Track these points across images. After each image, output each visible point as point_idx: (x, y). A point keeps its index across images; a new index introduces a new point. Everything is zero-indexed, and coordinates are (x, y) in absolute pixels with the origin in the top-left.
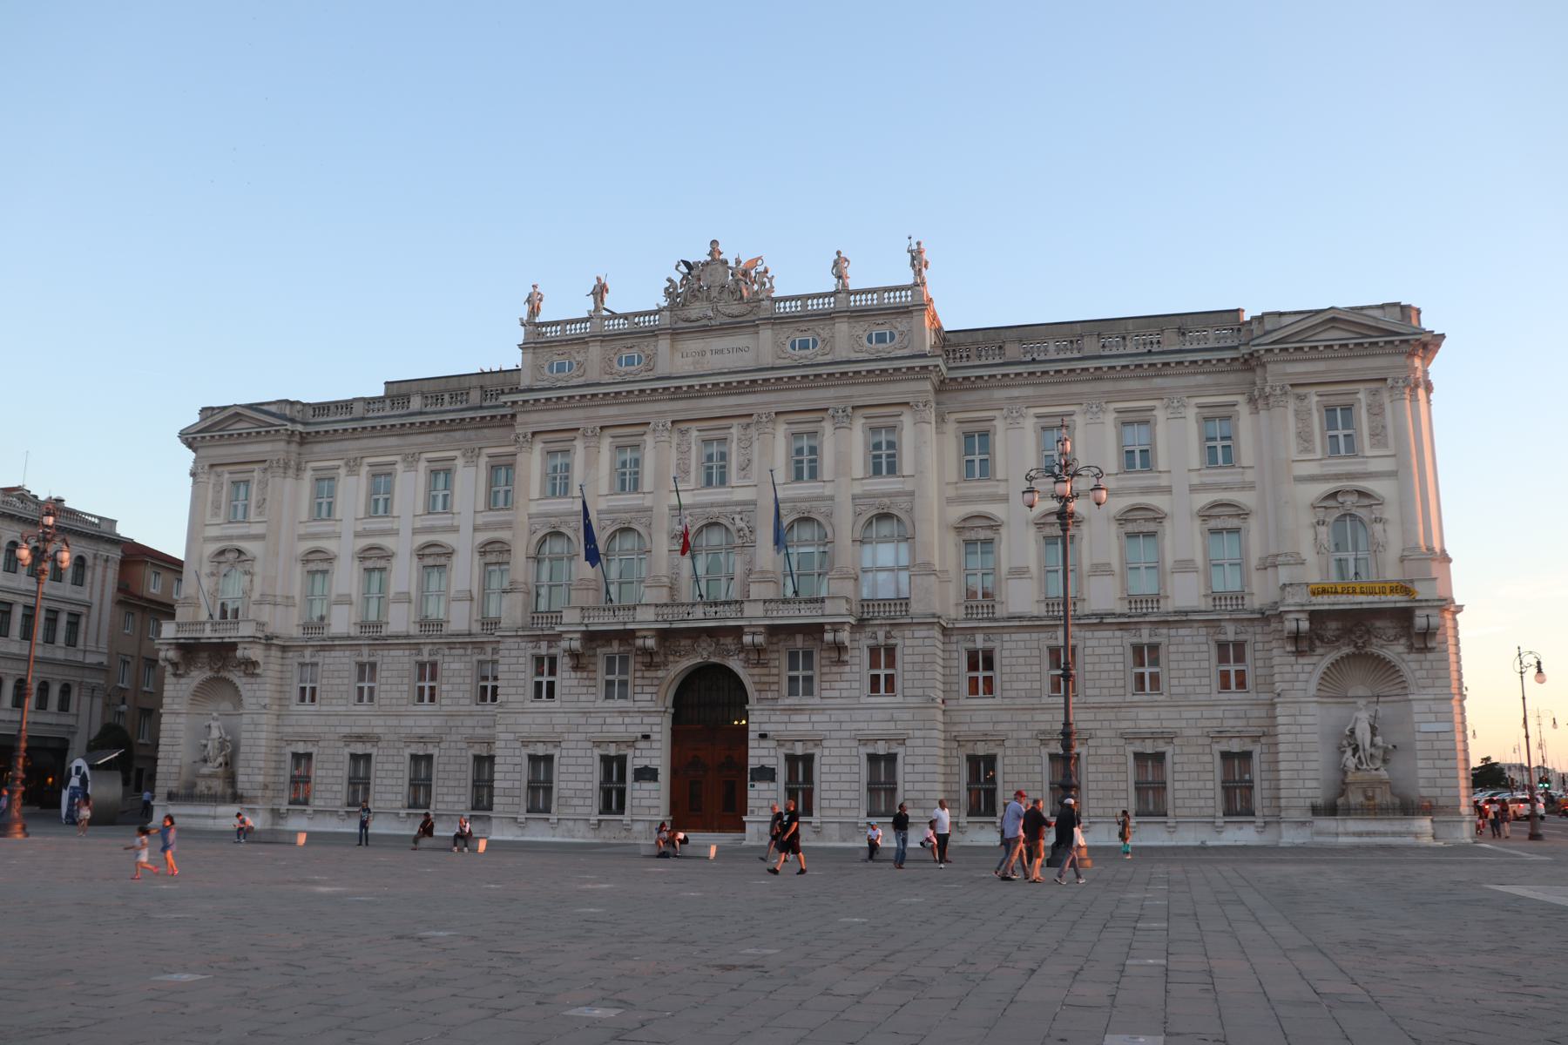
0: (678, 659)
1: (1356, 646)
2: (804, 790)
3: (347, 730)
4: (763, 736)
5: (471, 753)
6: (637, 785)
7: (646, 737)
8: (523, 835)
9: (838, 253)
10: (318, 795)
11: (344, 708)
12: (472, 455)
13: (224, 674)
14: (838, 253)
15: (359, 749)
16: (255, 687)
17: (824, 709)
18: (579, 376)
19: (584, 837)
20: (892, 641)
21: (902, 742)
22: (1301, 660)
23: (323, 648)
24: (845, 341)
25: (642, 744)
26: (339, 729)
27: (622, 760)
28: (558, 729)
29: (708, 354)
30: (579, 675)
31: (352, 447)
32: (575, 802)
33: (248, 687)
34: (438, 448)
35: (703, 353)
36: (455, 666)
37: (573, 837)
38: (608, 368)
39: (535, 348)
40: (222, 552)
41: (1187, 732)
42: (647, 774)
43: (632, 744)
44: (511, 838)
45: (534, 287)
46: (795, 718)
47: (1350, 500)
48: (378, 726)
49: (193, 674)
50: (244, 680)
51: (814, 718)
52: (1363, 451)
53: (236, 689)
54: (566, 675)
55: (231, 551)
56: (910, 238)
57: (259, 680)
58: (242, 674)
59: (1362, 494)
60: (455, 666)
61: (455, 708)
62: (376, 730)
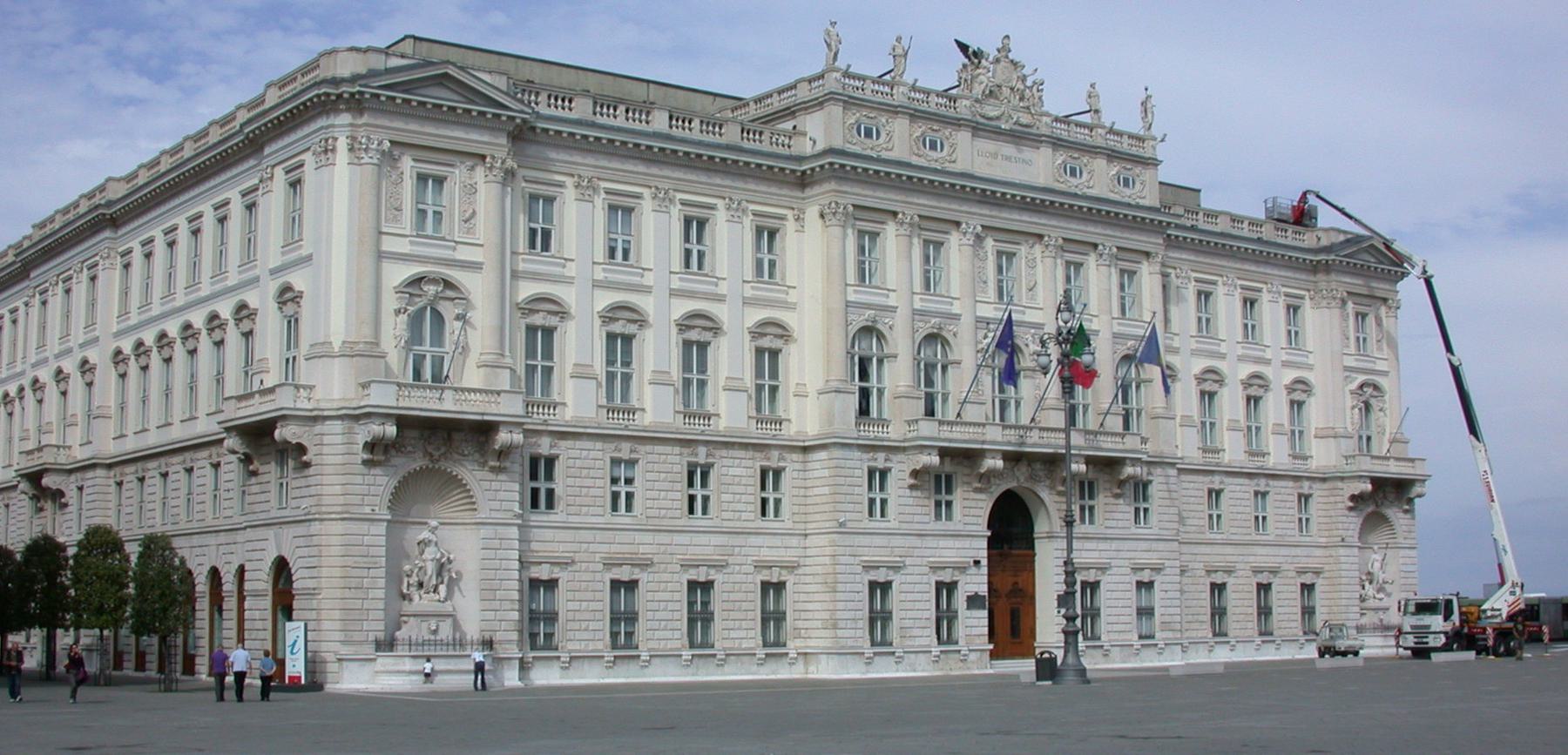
0: (998, 482)
1: (1377, 506)
2: (948, 617)
3: (605, 548)
5: (759, 578)
6: (968, 613)
7: (977, 563)
8: (868, 672)
9: (1092, 86)
10: (570, 635)
12: (663, 200)
13: (443, 465)
14: (1092, 86)
15: (624, 574)
17: (1106, 539)
18: (887, 150)
19: (923, 671)
20: (1150, 478)
21: (1229, 572)
22: (1352, 514)
23: (563, 435)
24: (1099, 179)
25: (973, 570)
26: (592, 547)
27: (951, 587)
29: (1000, 157)
30: (915, 493)
31: (587, 164)
32: (916, 632)
33: (486, 485)
34: (696, 189)
35: (995, 156)
36: (737, 471)
37: (915, 671)
38: (915, 148)
39: (845, 102)
40: (418, 281)
41: (1285, 567)
42: (973, 601)
43: (962, 569)
44: (857, 676)
45: (833, 24)
47: (1369, 390)
48: (645, 545)
52: (1372, 352)
54: (901, 492)
55: (434, 281)
56: (1146, 89)
59: (1376, 387)
60: (737, 471)
61: (738, 524)
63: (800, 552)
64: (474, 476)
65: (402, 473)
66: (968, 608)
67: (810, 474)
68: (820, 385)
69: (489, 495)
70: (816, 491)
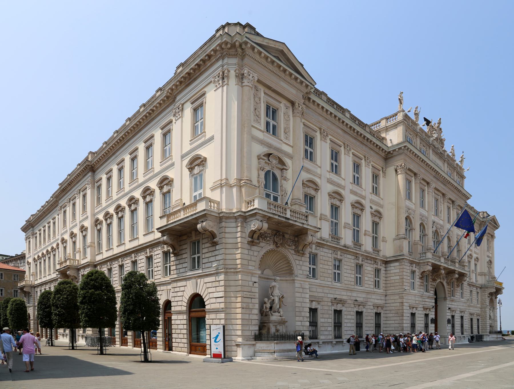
4: (449, 309)
11: (330, 283)
13: (280, 249)
16: (301, 263)
25: (432, 310)
28: (417, 302)
33: (297, 262)
36: (369, 269)
46: (453, 303)
48: (344, 295)
49: (262, 244)
50: (295, 257)
51: (455, 304)
53: (288, 263)
57: (303, 259)
58: (293, 252)
60: (369, 269)
62: (344, 297)
63: (383, 302)
64: (293, 257)
65: (264, 251)
66: (431, 323)
67: (389, 272)
68: (394, 236)
69: (299, 267)
70: (392, 278)
